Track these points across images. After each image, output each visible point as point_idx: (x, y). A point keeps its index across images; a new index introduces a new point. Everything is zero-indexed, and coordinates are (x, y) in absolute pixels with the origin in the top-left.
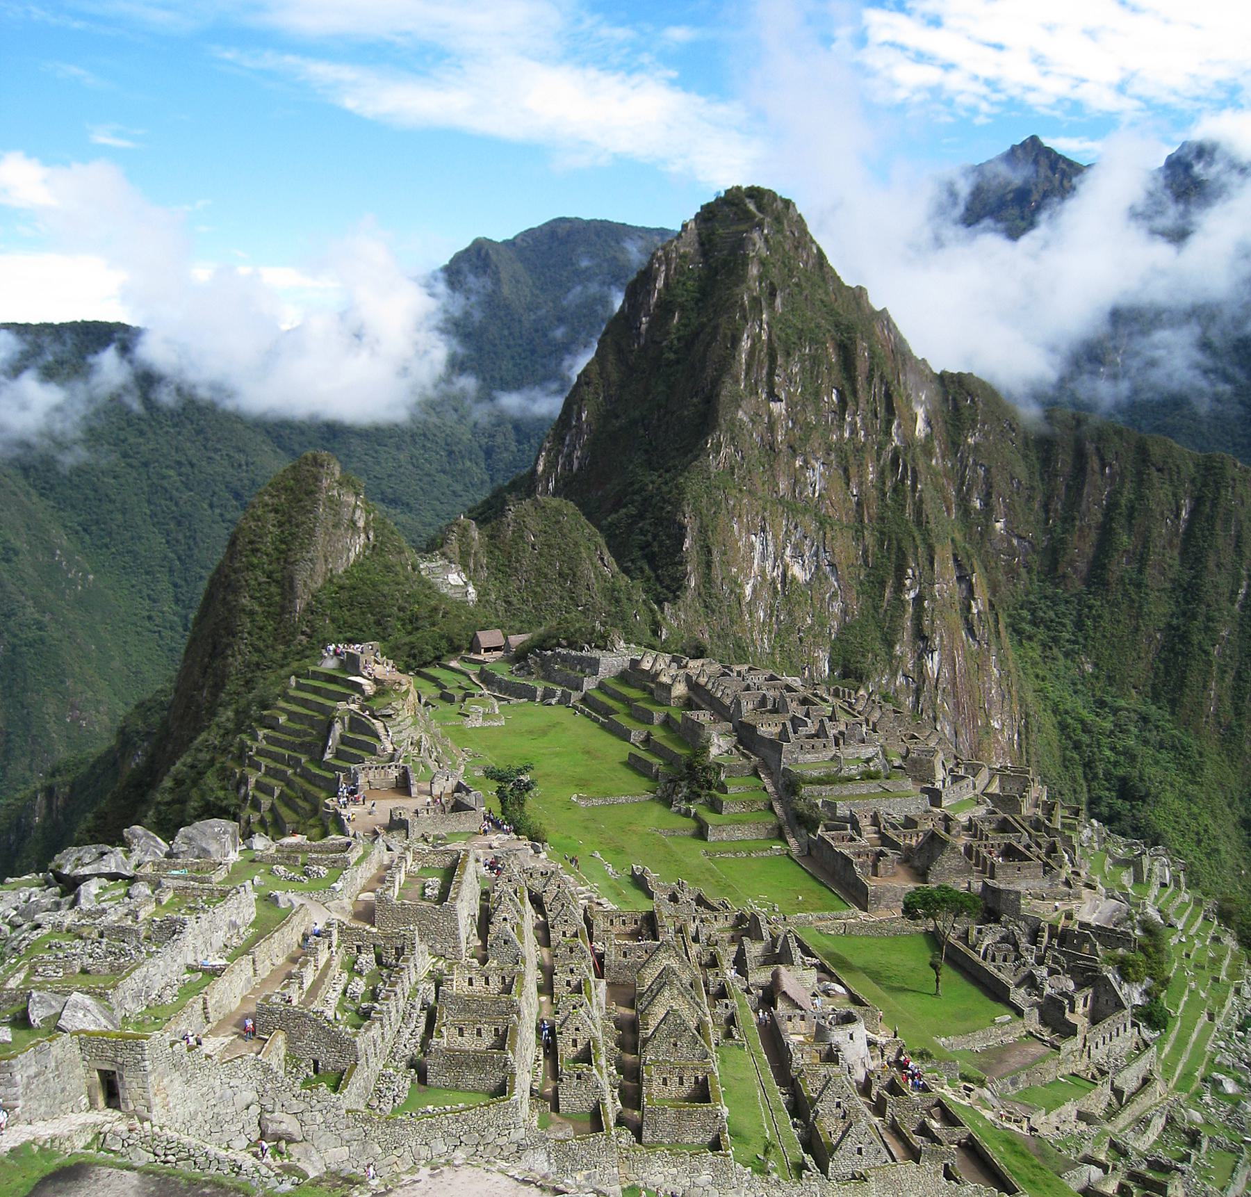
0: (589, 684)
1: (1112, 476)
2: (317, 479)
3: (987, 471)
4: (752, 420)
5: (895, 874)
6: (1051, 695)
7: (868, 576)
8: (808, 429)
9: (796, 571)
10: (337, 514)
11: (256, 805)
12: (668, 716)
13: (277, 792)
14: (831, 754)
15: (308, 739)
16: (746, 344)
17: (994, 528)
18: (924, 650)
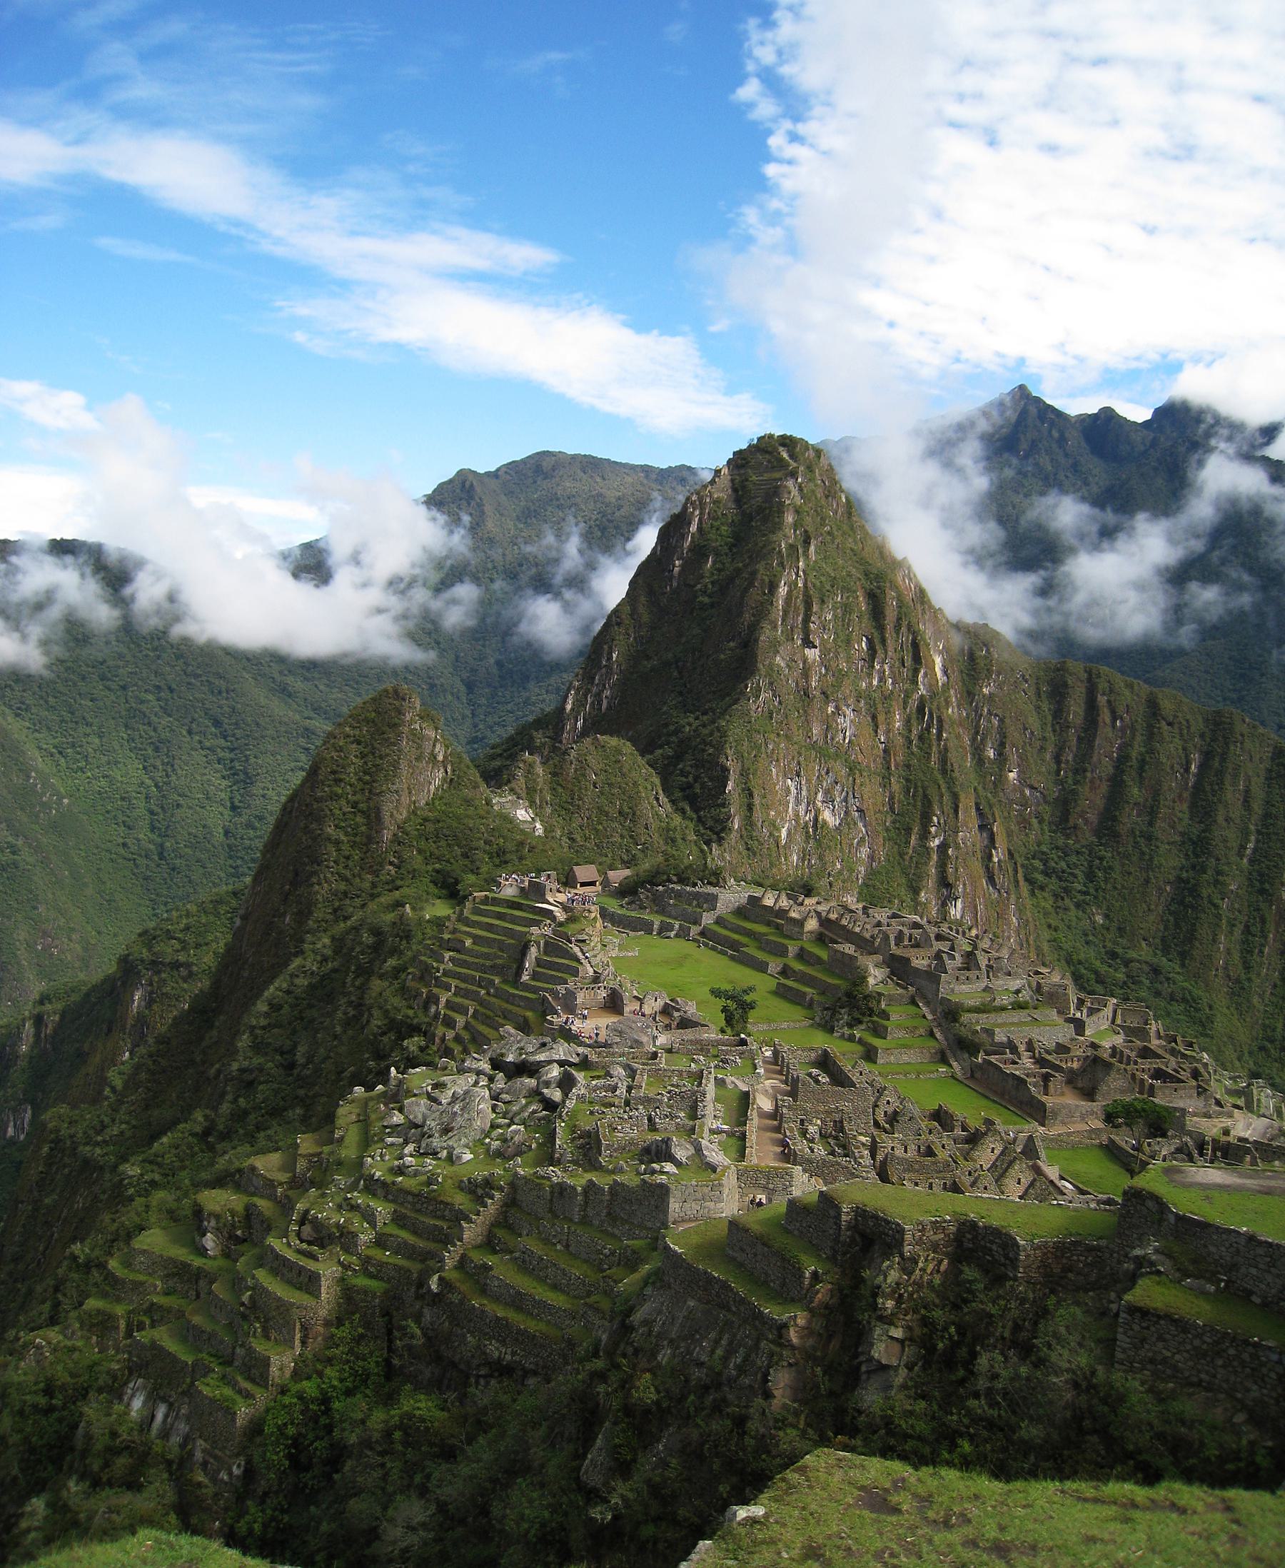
0: (708, 919)
1: (1123, 729)
2: (400, 712)
3: (1001, 721)
4: (788, 666)
5: (1062, 1094)
6: (1065, 946)
7: (894, 822)
8: (840, 676)
9: (827, 815)
10: (419, 747)
11: (450, 1023)
12: (802, 949)
13: (471, 1011)
14: (984, 985)
15: (499, 961)
16: (783, 590)
17: (1007, 777)
18: (948, 897)
